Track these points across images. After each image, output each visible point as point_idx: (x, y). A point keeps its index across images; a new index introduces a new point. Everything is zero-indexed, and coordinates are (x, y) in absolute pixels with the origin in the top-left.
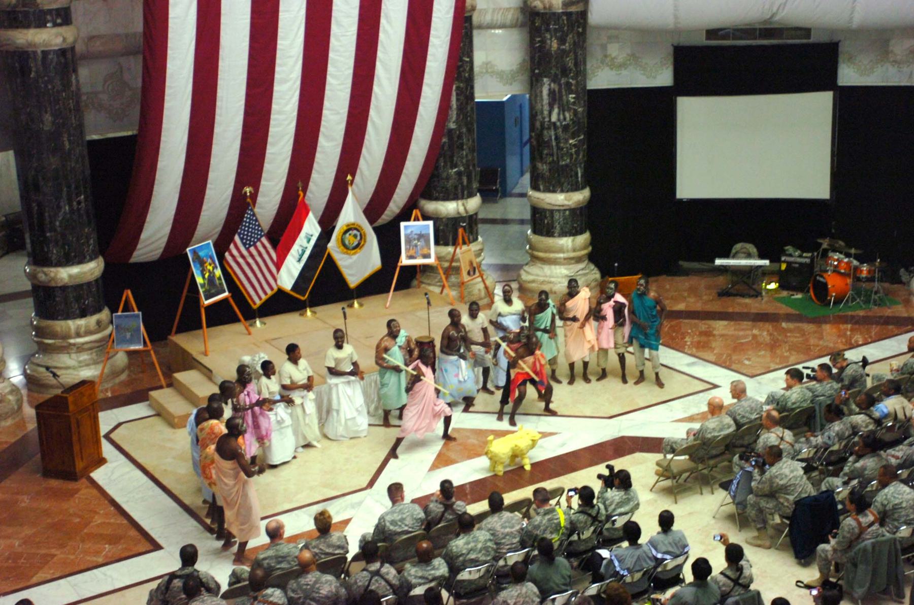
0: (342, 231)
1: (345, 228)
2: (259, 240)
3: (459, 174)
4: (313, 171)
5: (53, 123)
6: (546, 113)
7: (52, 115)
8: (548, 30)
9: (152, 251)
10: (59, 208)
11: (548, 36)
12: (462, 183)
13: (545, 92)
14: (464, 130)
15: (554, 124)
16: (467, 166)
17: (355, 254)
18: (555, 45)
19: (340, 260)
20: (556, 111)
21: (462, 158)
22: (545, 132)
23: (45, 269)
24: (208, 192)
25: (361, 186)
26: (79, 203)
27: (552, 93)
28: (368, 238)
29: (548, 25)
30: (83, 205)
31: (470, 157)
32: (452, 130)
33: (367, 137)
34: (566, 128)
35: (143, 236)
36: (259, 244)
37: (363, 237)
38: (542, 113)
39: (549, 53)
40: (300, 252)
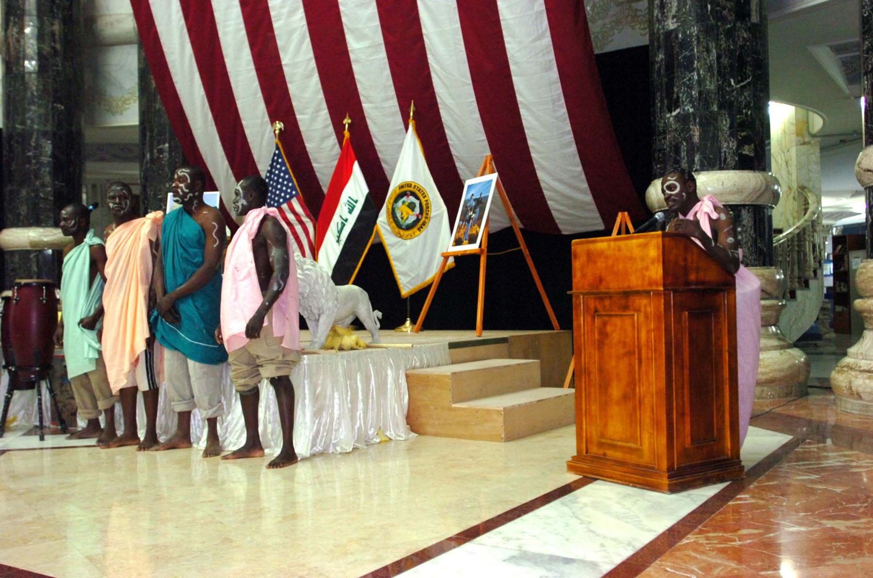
0: (394, 197)
1: (398, 192)
2: (288, 201)
3: (684, 119)
12: (689, 140)
14: (695, 30)
16: (704, 99)
17: (411, 237)
19: (393, 245)
21: (690, 87)
24: (248, 132)
25: (455, 128)
26: (161, 151)
28: (433, 214)
30: (166, 154)
31: (711, 85)
32: (671, 31)
33: (424, 31)
36: (285, 206)
37: (424, 210)
40: (340, 226)
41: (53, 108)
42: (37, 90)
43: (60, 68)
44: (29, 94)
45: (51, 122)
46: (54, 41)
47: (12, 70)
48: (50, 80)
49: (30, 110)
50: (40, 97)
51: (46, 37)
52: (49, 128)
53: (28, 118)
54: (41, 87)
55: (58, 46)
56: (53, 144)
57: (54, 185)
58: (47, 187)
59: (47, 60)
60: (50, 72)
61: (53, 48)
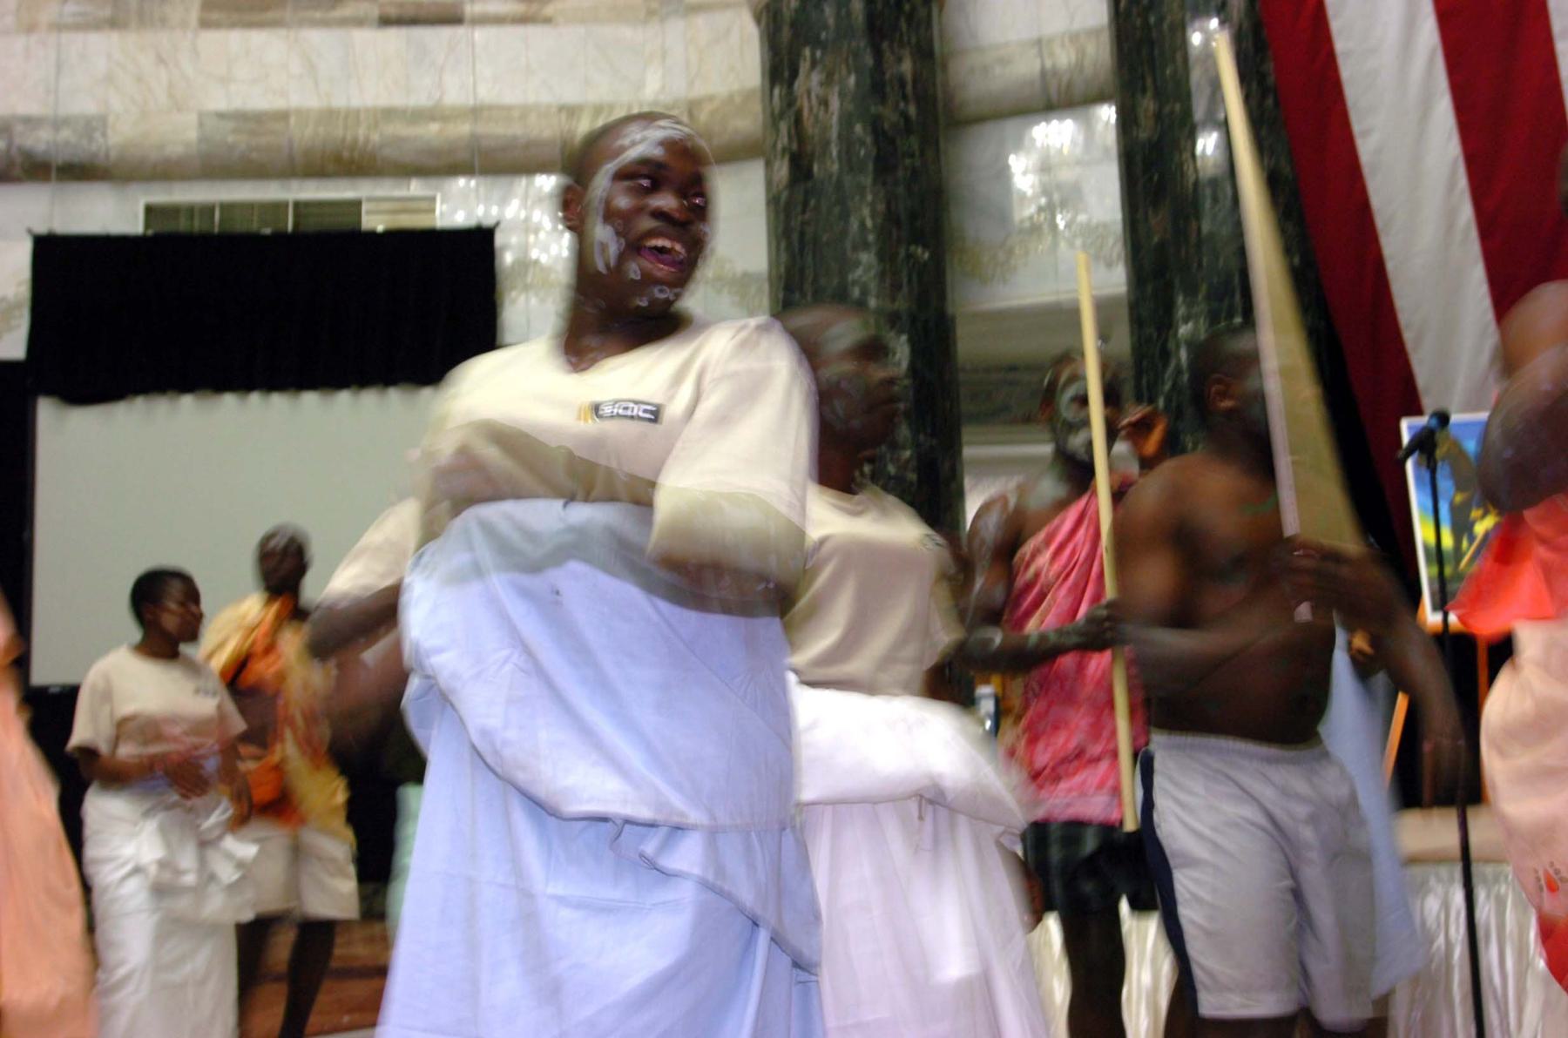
5: (1158, 116)
7: (1159, 95)
10: (1165, 355)
41: (909, 256)
42: (873, 216)
43: (918, 163)
44: (854, 225)
45: (905, 289)
46: (905, 97)
47: (809, 174)
48: (901, 190)
49: (857, 264)
50: (883, 233)
51: (888, 89)
52: (902, 304)
53: (854, 283)
54: (881, 207)
55: (912, 110)
56: (911, 341)
57: (917, 445)
58: (904, 448)
59: (892, 142)
60: (900, 173)
61: (905, 115)
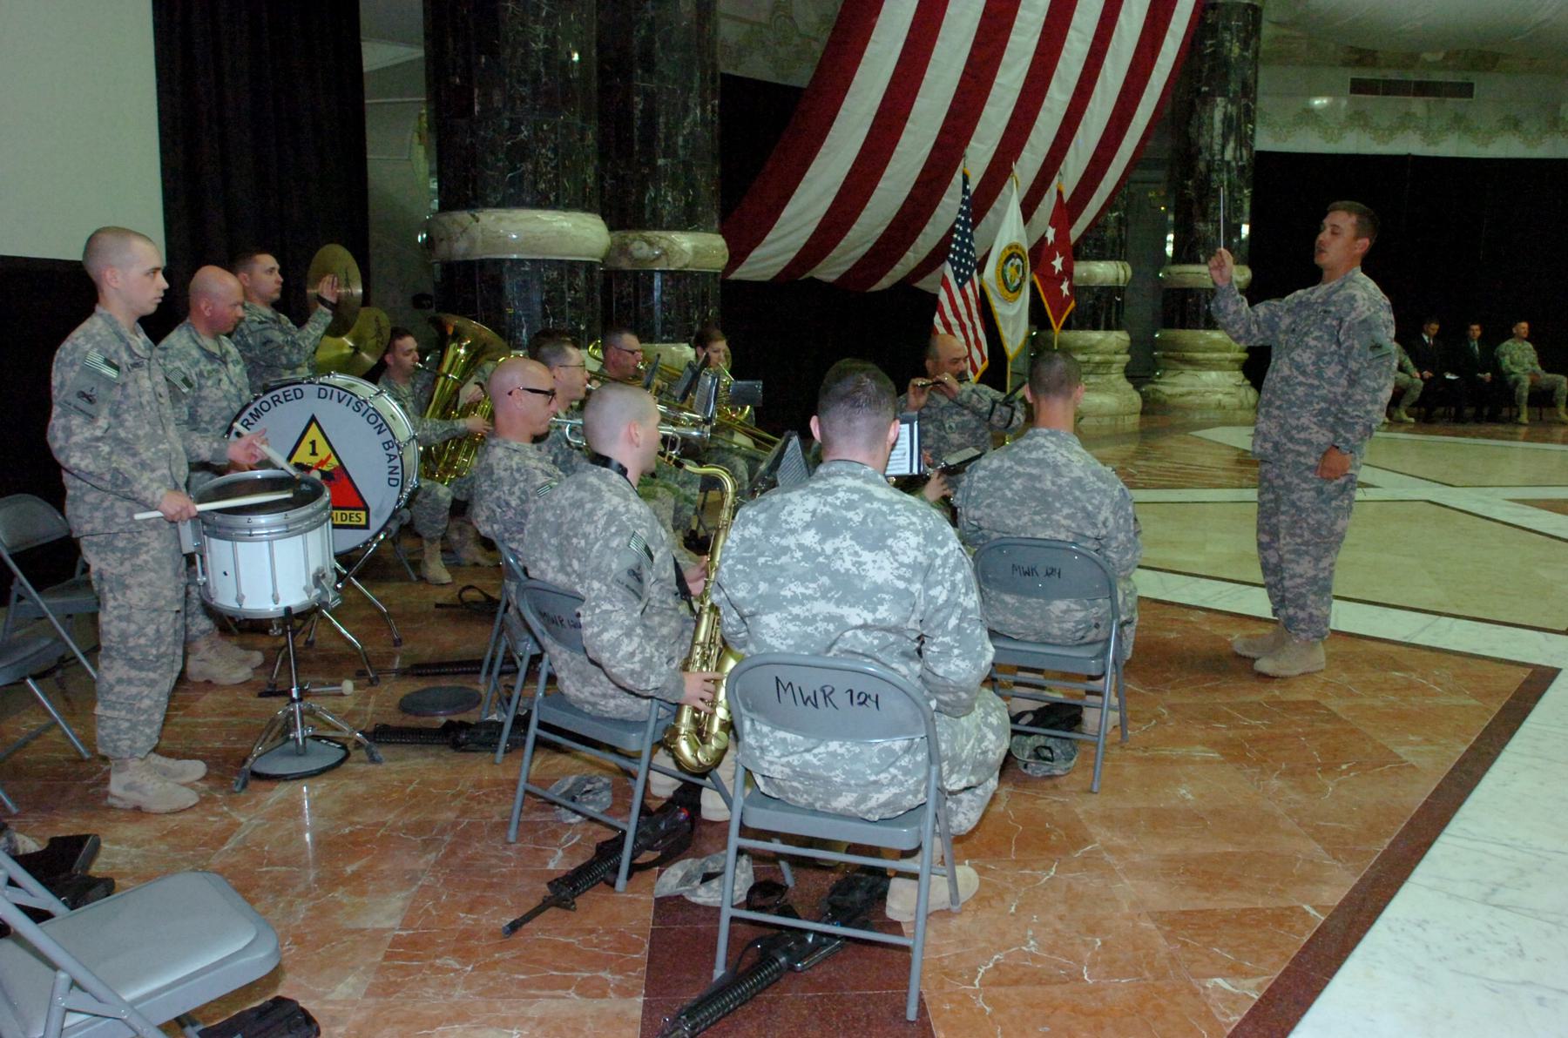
4: (1027, 146)
6: (1217, 148)
8: (1227, 28)
9: (765, 259)
11: (1227, 36)
13: (1218, 115)
15: (1228, 163)
18: (1236, 50)
20: (1232, 144)
22: (1214, 176)
23: (648, 234)
27: (1227, 120)
29: (1229, 20)
34: (1241, 169)
35: (787, 213)
38: (1210, 148)
39: (1226, 63)
